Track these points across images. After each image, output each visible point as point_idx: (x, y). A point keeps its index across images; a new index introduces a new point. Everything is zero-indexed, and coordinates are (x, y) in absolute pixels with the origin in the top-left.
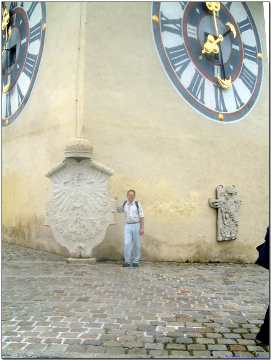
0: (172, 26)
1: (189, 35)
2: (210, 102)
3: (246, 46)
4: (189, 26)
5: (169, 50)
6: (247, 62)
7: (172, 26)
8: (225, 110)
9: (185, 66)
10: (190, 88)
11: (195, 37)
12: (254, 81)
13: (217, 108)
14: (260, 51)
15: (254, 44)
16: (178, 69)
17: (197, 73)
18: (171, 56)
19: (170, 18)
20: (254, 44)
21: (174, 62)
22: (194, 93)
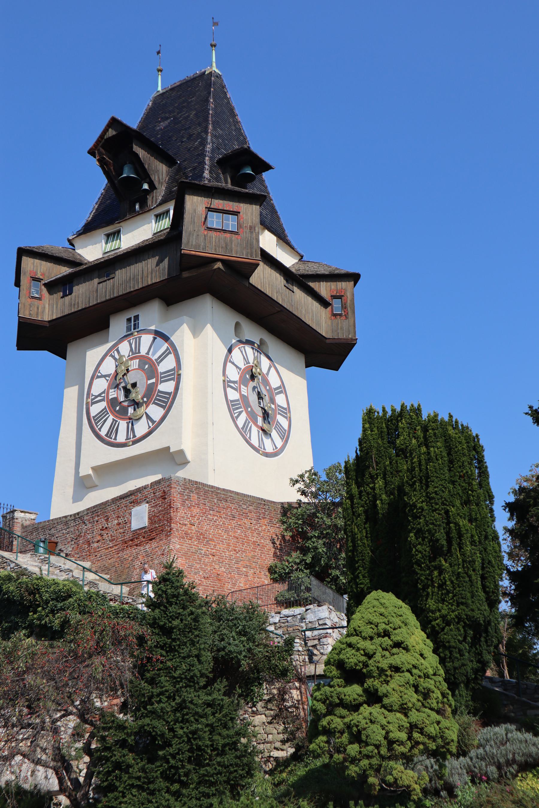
0: (232, 385)
1: (242, 393)
2: (255, 441)
3: (279, 406)
4: (242, 386)
5: (232, 401)
6: (280, 418)
7: (232, 385)
8: (264, 449)
9: (240, 413)
10: (243, 428)
11: (246, 394)
12: (285, 434)
13: (259, 446)
14: (290, 412)
15: (285, 406)
16: (236, 415)
17: (247, 419)
18: (233, 405)
19: (232, 379)
20: (285, 406)
21: (234, 410)
22: (245, 432)
